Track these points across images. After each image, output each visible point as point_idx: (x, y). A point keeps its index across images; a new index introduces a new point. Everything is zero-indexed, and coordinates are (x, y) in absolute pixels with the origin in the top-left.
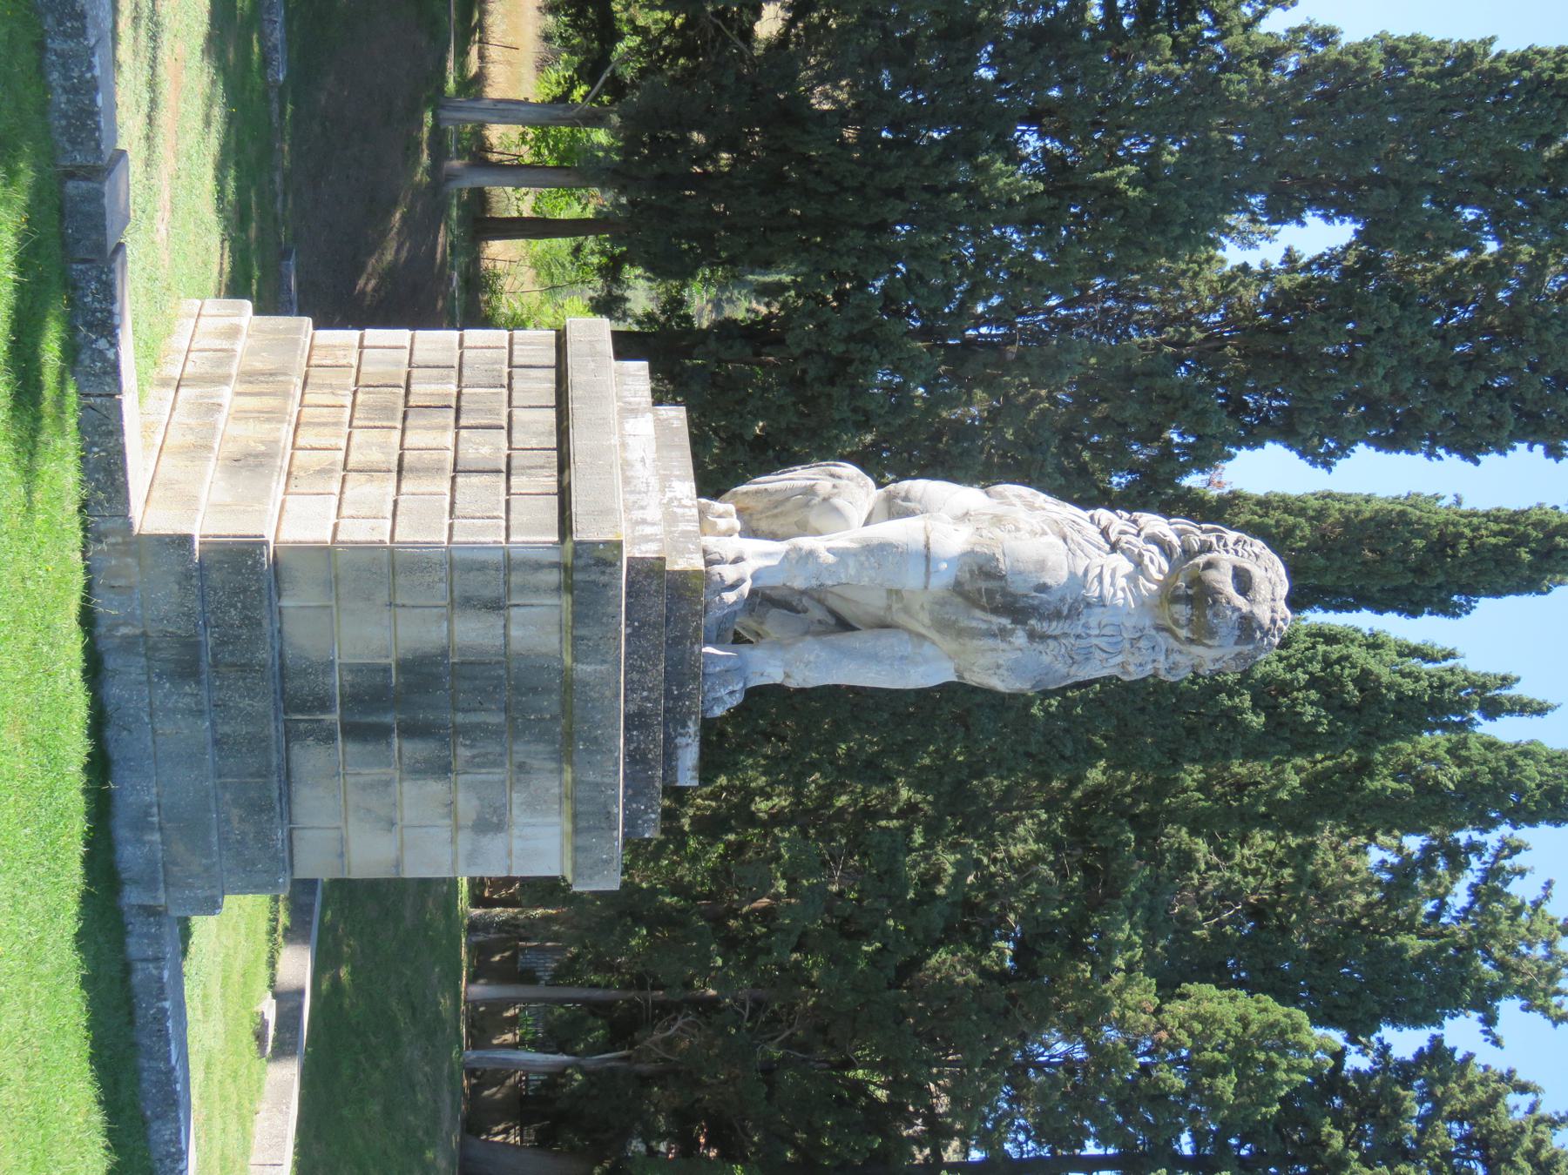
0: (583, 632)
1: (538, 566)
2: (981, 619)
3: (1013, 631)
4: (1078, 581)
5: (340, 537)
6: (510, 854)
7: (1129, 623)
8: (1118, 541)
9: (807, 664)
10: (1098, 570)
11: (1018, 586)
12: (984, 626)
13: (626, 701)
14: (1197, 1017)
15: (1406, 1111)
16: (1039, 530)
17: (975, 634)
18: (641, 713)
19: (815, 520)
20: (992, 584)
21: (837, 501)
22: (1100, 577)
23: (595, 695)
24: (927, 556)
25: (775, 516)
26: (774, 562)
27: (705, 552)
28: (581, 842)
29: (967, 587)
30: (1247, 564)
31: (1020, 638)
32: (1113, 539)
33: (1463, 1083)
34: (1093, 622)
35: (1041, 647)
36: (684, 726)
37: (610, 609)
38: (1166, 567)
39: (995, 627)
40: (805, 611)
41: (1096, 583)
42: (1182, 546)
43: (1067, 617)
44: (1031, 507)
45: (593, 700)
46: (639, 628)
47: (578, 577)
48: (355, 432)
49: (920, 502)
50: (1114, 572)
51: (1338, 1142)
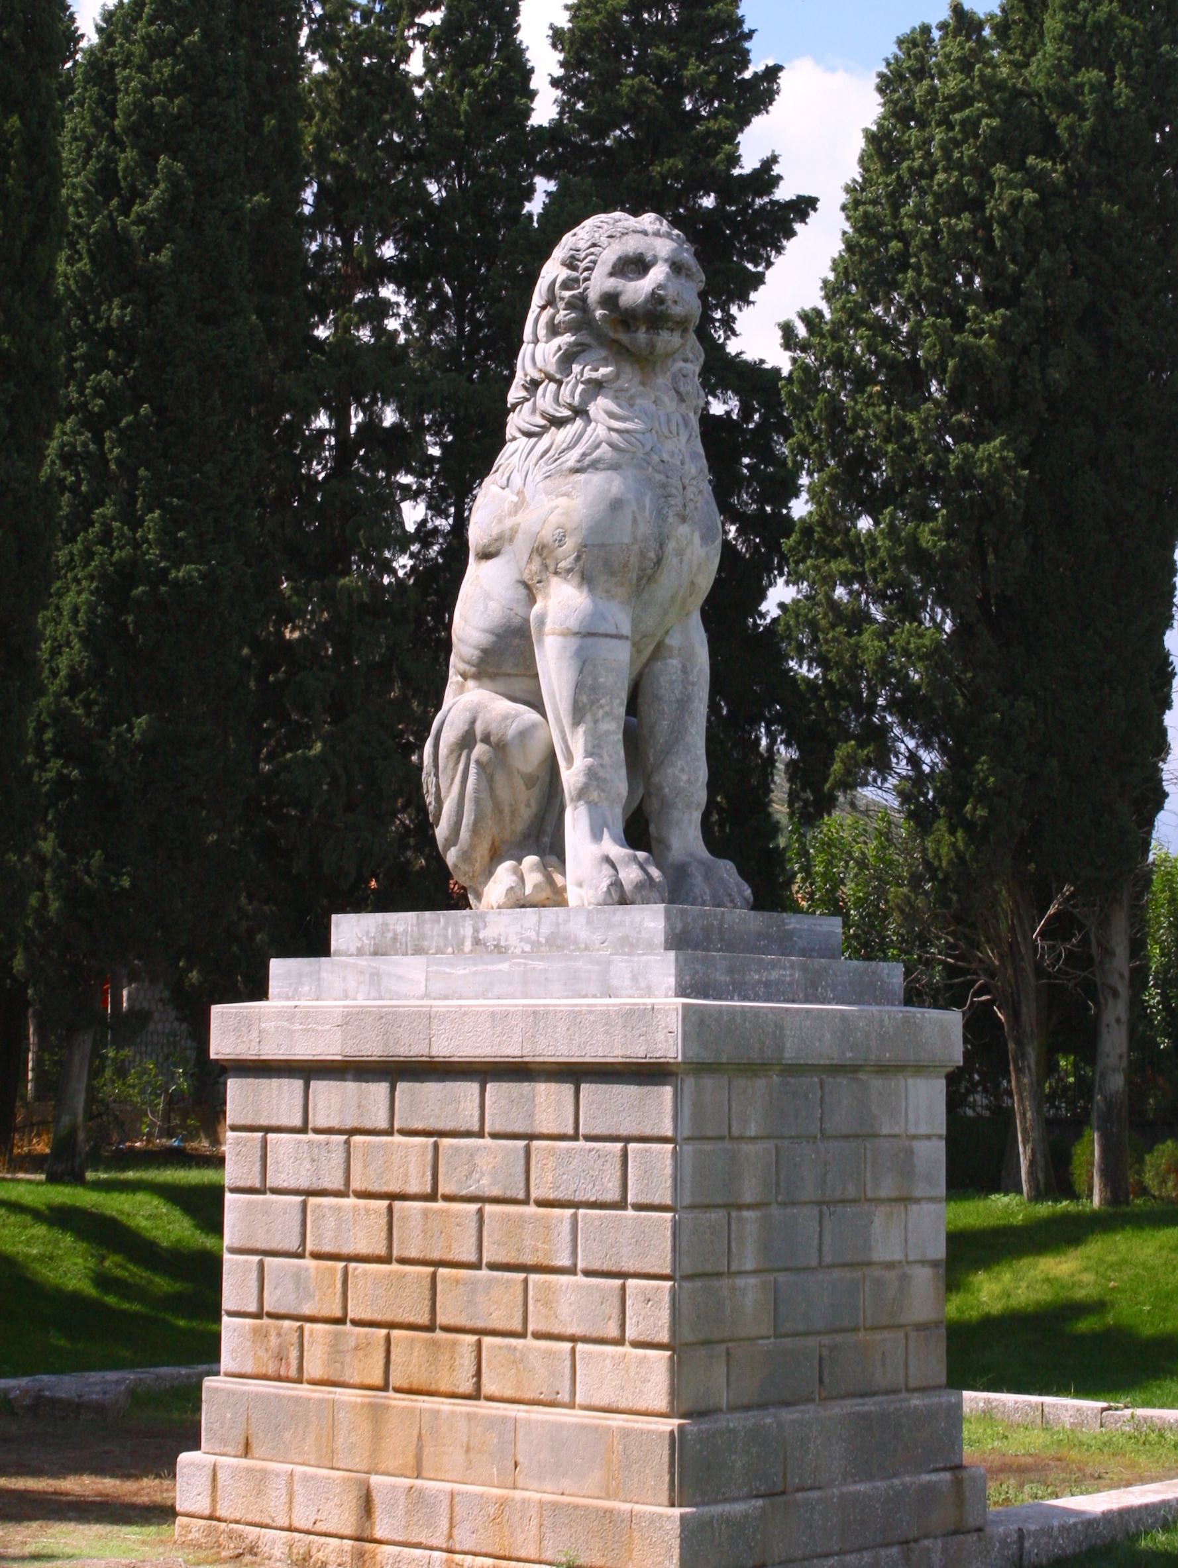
1: (698, 1105)
5: (664, 1337)
6: (928, 1137)
8: (570, 407)
13: (793, 1001)
32: (567, 413)
48: (441, 1319)
50: (611, 415)
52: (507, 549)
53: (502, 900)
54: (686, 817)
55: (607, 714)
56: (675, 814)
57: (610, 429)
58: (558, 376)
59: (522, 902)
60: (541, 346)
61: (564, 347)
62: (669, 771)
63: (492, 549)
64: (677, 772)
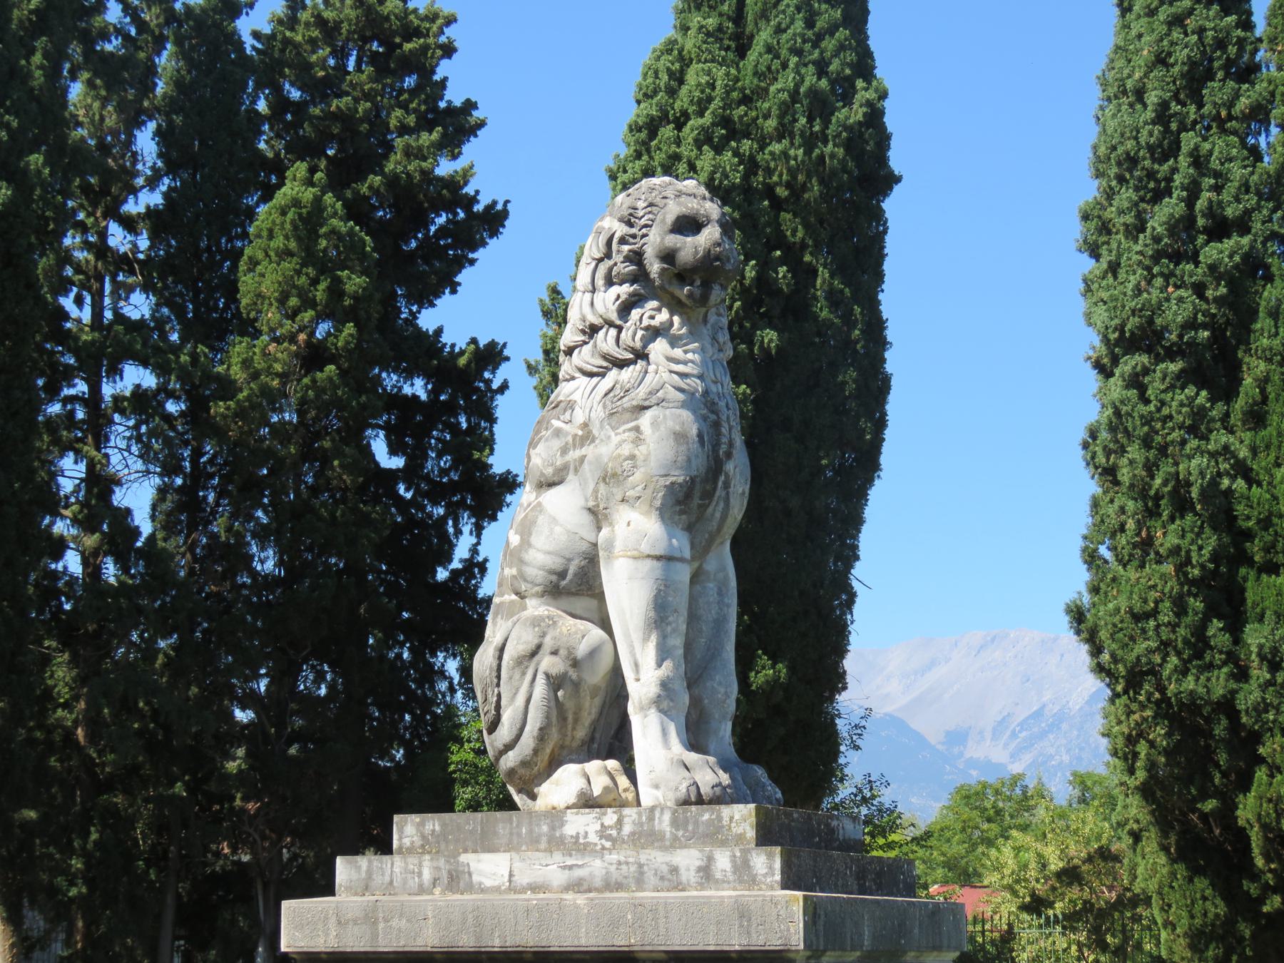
4: (690, 401)
7: (710, 351)
8: (633, 350)
10: (675, 376)
11: (700, 465)
12: (722, 505)
14: (283, 300)
15: (349, 109)
16: (632, 435)
19: (597, 675)
20: (698, 487)
21: (582, 650)
22: (683, 375)
24: (667, 559)
25: (576, 720)
26: (672, 729)
27: (686, 802)
29: (693, 519)
30: (670, 216)
33: (308, 48)
38: (654, 304)
39: (724, 494)
41: (688, 381)
42: (633, 282)
43: (718, 415)
44: (587, 437)
46: (816, 877)
49: (569, 560)
51: (377, 180)
52: (571, 477)
53: (572, 800)
54: (723, 727)
55: (674, 630)
57: (671, 372)
58: (619, 322)
59: (591, 802)
60: (599, 297)
61: (623, 297)
62: (709, 684)
63: (556, 479)
64: (715, 685)
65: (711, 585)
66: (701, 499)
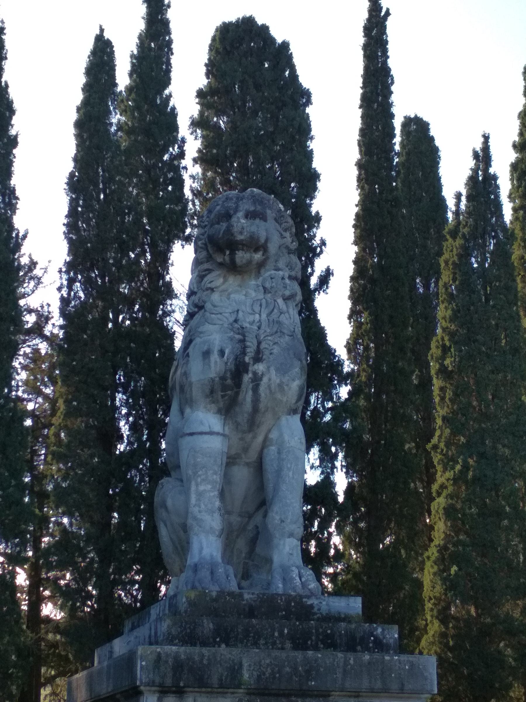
0: (215, 680)
2: (247, 396)
3: (255, 373)
9: (282, 521)
12: (250, 393)
17: (256, 400)
18: (292, 638)
23: (269, 670)
28: (395, 686)
31: (260, 368)
34: (251, 318)
35: (267, 352)
36: (312, 606)
37: (197, 658)
38: (217, 273)
40: (257, 527)
43: (244, 336)
45: (273, 673)
47: (169, 682)
56: (276, 541)
64: (274, 515)
65: (273, 448)
66: (222, 392)
